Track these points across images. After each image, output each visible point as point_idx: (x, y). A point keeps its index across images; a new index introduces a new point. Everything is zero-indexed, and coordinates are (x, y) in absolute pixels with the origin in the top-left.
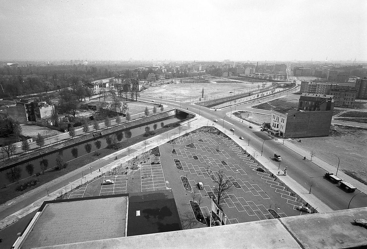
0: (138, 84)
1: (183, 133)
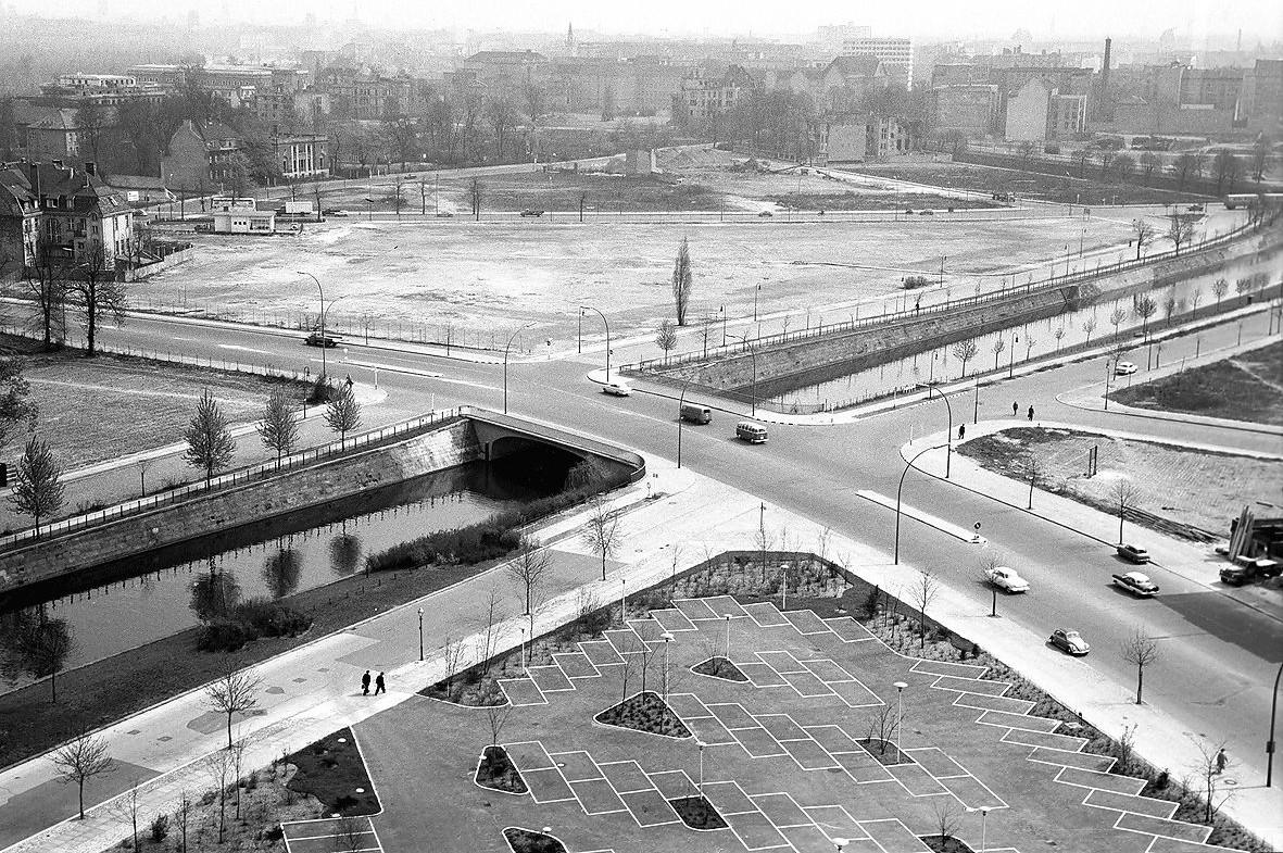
0: (88, 207)
1: (563, 609)
